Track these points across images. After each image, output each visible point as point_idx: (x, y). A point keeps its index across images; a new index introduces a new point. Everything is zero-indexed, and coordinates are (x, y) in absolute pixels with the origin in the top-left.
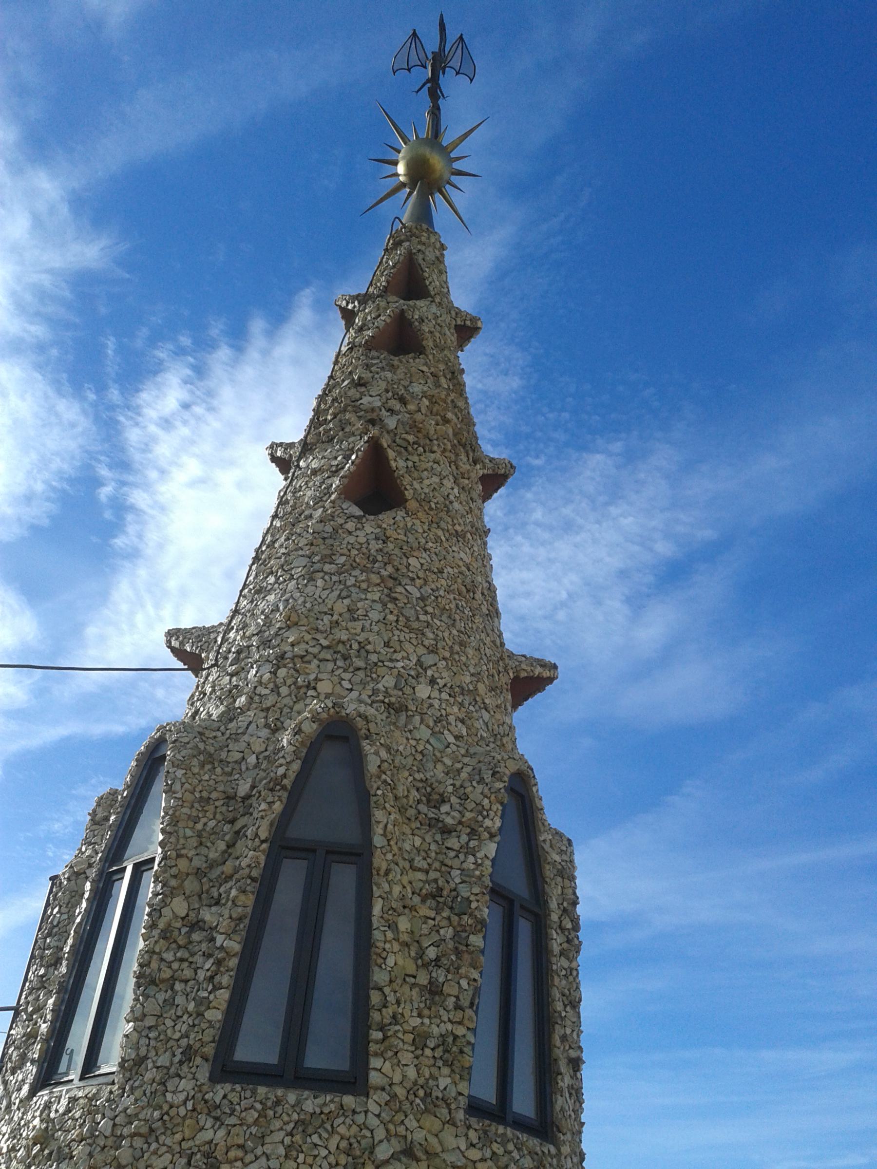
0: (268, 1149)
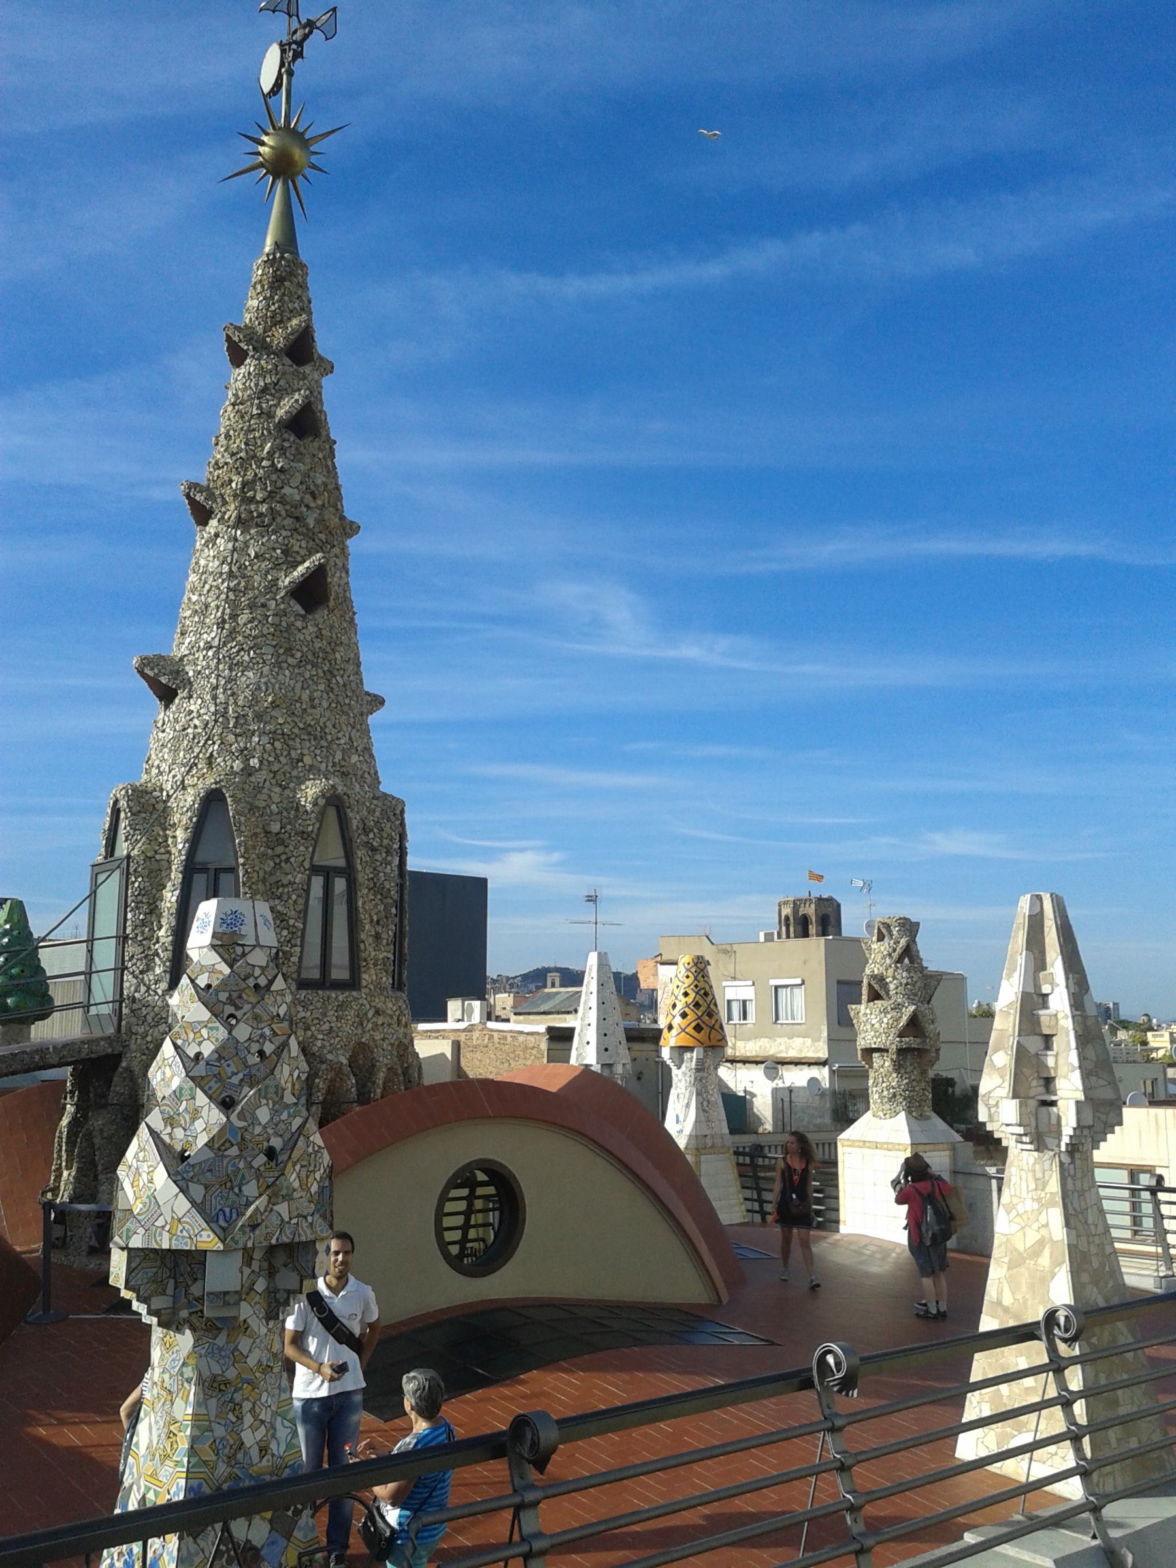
0: (329, 1019)
